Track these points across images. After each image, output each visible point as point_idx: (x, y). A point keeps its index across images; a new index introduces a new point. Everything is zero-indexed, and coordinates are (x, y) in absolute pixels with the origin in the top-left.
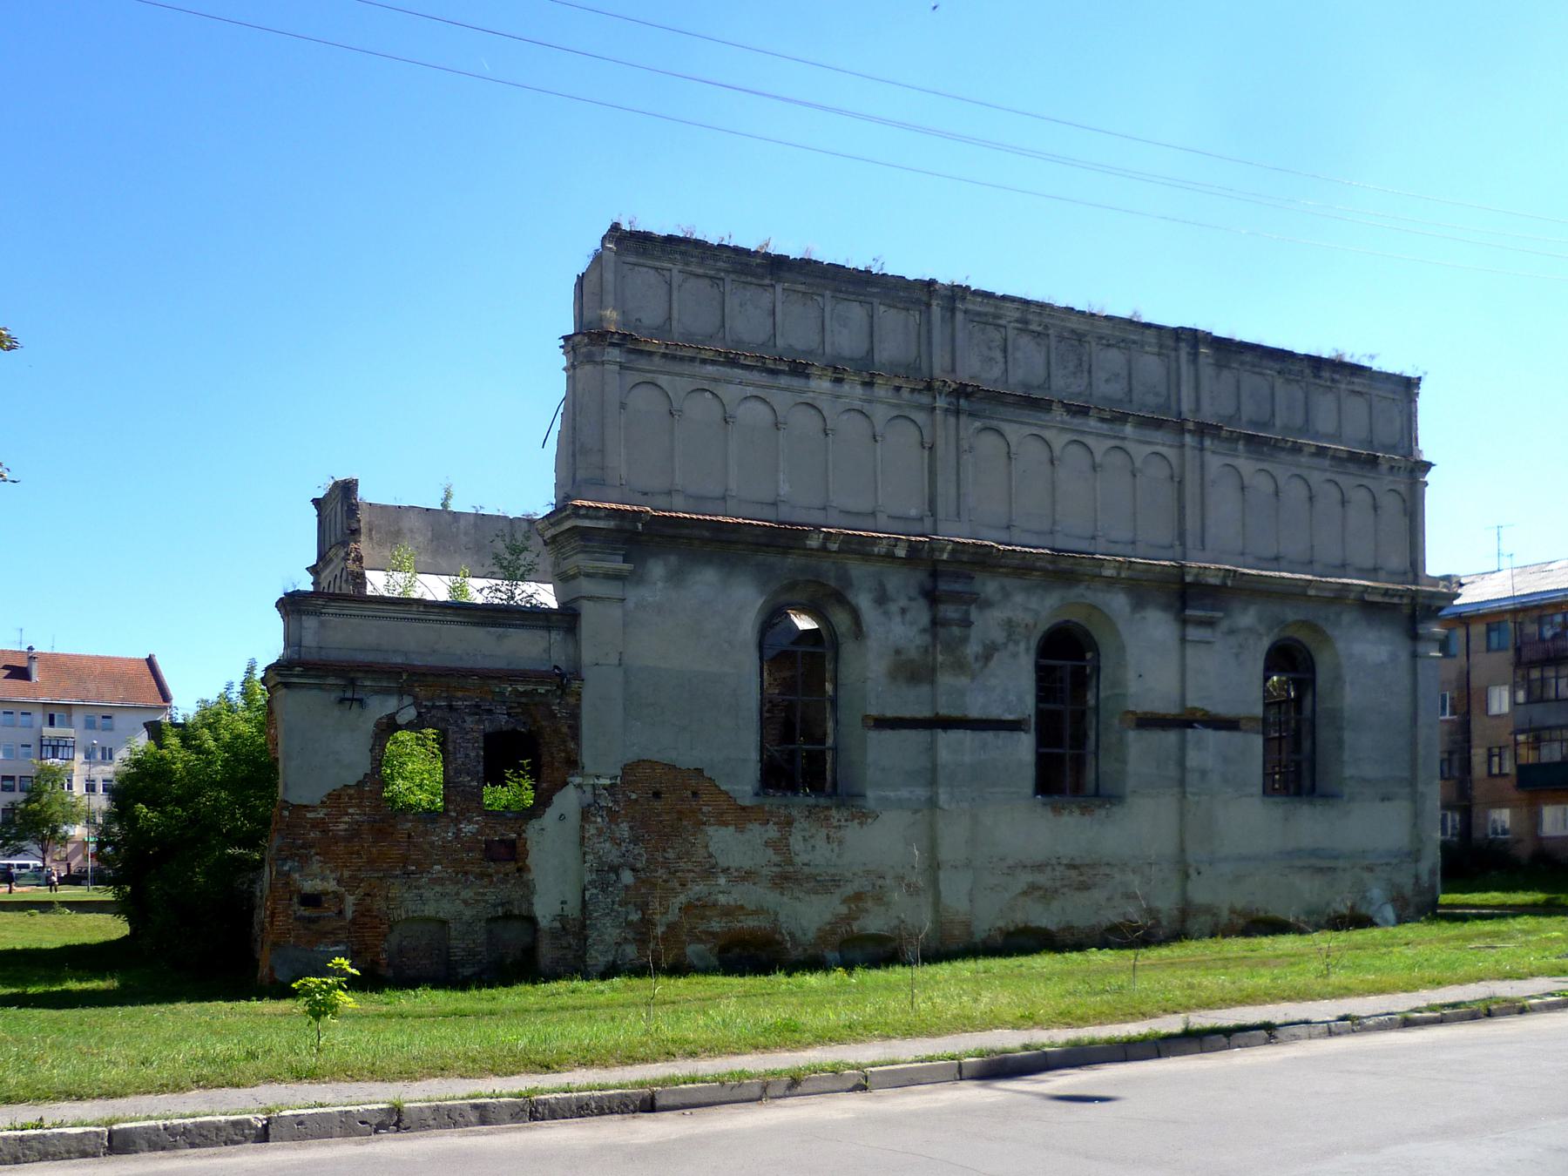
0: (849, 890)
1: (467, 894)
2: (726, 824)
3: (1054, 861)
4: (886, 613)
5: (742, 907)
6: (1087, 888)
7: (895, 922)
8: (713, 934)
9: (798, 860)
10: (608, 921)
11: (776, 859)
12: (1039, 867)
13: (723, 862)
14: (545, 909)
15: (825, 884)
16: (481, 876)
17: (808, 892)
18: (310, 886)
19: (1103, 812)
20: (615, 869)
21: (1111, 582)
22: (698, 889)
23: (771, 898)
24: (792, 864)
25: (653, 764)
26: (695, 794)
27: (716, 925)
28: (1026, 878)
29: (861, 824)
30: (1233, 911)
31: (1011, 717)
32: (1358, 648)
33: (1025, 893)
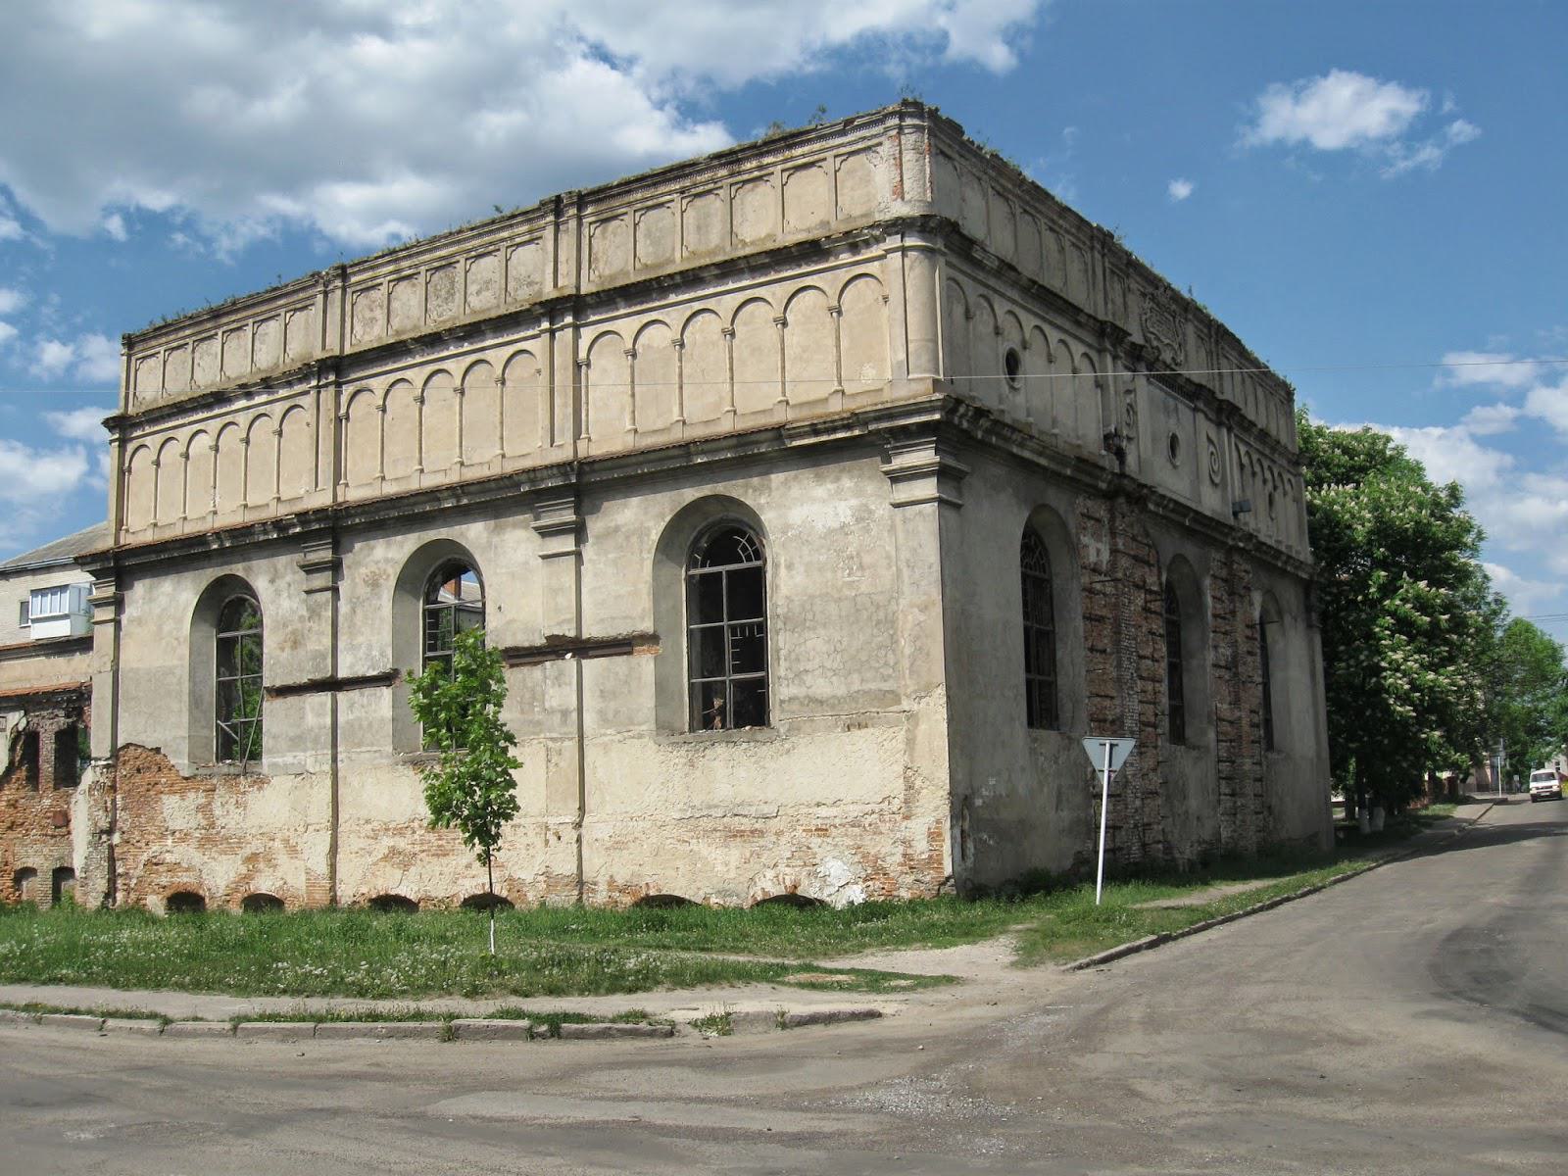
0: (248, 851)
1: (46, 851)
3: (416, 824)
4: (278, 593)
7: (282, 882)
9: (218, 823)
10: (98, 873)
11: (204, 823)
13: (172, 825)
14: (78, 863)
16: (53, 836)
20: (110, 832)
21: (464, 514)
24: (212, 825)
27: (164, 880)
28: (387, 842)
31: (375, 673)
32: (797, 515)
33: (385, 858)
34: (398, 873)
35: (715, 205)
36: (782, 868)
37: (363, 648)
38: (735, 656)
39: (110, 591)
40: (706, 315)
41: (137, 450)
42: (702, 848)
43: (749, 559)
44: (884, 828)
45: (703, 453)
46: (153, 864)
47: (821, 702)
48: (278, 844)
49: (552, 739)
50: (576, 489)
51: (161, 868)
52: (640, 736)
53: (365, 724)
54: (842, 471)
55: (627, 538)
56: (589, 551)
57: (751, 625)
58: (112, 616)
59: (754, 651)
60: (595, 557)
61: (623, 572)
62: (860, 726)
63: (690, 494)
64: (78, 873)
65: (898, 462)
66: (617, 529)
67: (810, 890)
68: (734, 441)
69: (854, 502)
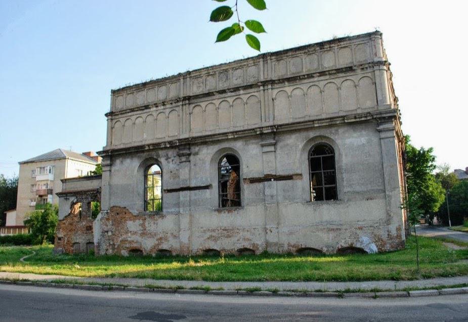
2: (131, 220)
3: (219, 228)
4: (169, 162)
5: (133, 241)
6: (230, 237)
7: (170, 246)
8: (128, 248)
11: (142, 229)
12: (214, 231)
13: (130, 230)
14: (95, 241)
15: (152, 235)
17: (148, 238)
18: (60, 236)
19: (236, 212)
20: (107, 232)
22: (124, 236)
23: (140, 239)
25: (116, 207)
26: (125, 213)
27: (127, 246)
28: (208, 234)
29: (162, 219)
30: (289, 245)
31: (204, 185)
33: (208, 238)
34: (213, 243)
35: (315, 57)
36: (347, 239)
37: (199, 178)
38: (325, 180)
39: (108, 162)
40: (315, 87)
41: (116, 122)
42: (320, 234)
43: (329, 153)
44: (381, 227)
45: (318, 123)
46: (123, 241)
47: (358, 193)
48: (169, 235)
49: (267, 204)
50: (273, 135)
51: (126, 242)
52: (297, 203)
53: (201, 200)
54: (362, 129)
55: (291, 147)
56: (278, 151)
57: (330, 172)
58: (109, 169)
59: (332, 179)
60: (281, 153)
61: (293, 156)
62: (371, 199)
63: (312, 134)
64: (95, 244)
65: (381, 127)
66: (288, 145)
67: (358, 246)
68: (329, 120)
69: (367, 138)
